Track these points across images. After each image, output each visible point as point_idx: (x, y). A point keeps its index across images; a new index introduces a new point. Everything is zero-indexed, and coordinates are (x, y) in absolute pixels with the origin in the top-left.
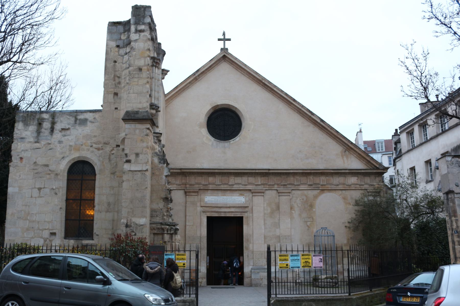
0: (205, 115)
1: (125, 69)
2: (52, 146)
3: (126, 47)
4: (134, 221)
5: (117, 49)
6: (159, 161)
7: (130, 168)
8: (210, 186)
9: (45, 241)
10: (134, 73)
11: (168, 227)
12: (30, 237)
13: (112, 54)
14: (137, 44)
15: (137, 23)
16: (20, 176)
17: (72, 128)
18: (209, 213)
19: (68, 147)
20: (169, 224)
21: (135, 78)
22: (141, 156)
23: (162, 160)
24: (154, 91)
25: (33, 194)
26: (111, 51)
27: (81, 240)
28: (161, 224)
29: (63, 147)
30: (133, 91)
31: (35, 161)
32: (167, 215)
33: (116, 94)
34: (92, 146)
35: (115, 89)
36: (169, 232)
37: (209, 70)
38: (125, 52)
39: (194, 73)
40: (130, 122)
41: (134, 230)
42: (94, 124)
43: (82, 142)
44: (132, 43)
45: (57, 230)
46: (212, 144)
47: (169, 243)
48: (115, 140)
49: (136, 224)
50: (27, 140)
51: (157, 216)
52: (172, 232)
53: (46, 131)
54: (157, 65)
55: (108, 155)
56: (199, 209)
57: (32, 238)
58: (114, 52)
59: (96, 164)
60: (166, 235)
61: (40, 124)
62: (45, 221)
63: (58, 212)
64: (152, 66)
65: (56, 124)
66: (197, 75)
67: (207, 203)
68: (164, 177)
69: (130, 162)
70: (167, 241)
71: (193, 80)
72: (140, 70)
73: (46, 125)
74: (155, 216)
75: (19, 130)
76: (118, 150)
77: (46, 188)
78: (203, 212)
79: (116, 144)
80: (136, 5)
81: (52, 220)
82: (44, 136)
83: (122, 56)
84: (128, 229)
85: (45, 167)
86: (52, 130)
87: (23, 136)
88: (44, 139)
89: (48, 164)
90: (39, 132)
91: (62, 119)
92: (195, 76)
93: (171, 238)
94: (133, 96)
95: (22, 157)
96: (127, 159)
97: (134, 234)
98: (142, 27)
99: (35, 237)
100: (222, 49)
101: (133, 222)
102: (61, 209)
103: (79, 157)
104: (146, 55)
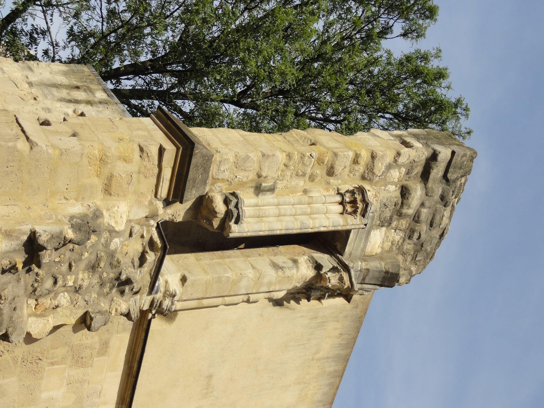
50: (29, 74)
54: (349, 208)
73: (80, 95)
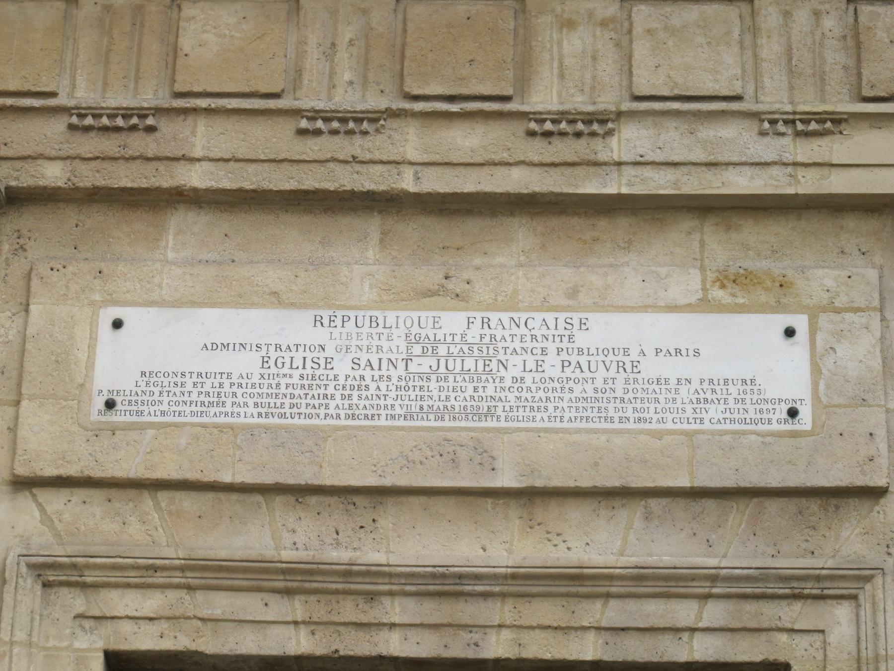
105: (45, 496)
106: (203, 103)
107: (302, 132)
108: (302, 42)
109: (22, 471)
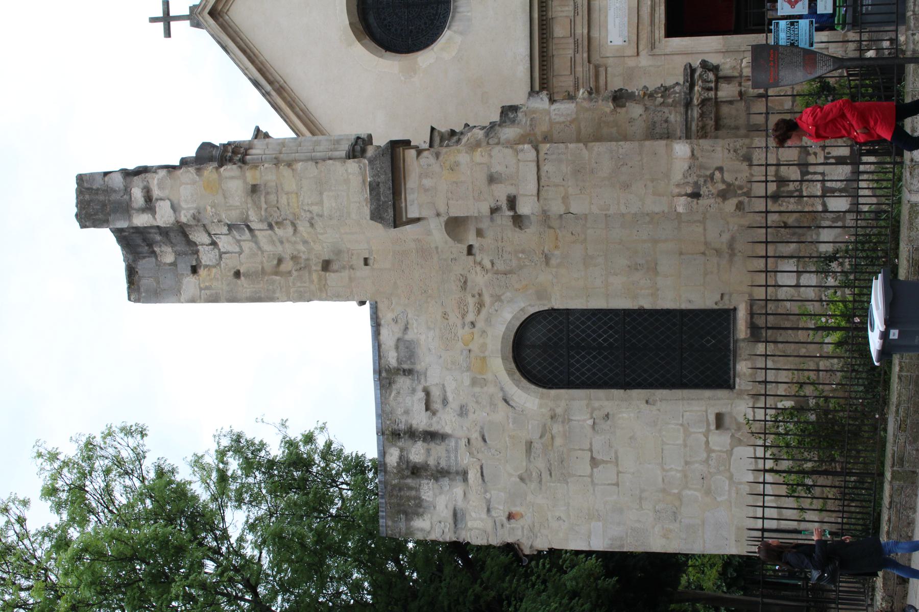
0: (380, 59)
1: (256, 243)
2: (475, 436)
3: (195, 244)
4: (681, 176)
5: (202, 272)
6: (508, 123)
7: (532, 195)
8: (579, 31)
9: (740, 442)
10: (264, 206)
11: (696, 88)
12: (729, 485)
13: (215, 284)
14: (184, 205)
15: (125, 209)
16: (559, 518)
17: (423, 381)
18: (657, 32)
19: (477, 389)
20: (688, 84)
21: (277, 201)
22: (497, 168)
23: (507, 114)
24: (313, 154)
25: (610, 482)
26: (207, 288)
27: (736, 341)
28: (688, 104)
29: (477, 402)
30: (317, 204)
31: (518, 480)
32: (662, 97)
33: (326, 265)
34: (473, 324)
35: (314, 268)
36: (713, 85)
37: (254, 55)
38: (210, 247)
39: (263, 95)
40: (401, 208)
41: (708, 173)
42: (410, 321)
43: (462, 351)
44: (184, 219)
45: (709, 411)
46: (461, 33)
47: (743, 84)
48: (456, 259)
49: (690, 168)
50: (460, 504)
51: (666, 121)
52: (711, 76)
53: (433, 452)
55: (496, 276)
56: (645, 60)
57: (731, 478)
58: (211, 279)
59: (522, 310)
60: (720, 94)
61: (416, 471)
62: (685, 446)
63: (659, 410)
64: (243, 161)
65: (414, 426)
66: (268, 88)
67: (627, 39)
68: (556, 106)
69: (515, 197)
70: (739, 89)
71: (284, 99)
72: (254, 189)
73: (417, 453)
74: (665, 125)
75: (432, 527)
76: (482, 249)
77: (591, 444)
78: (653, 46)
79: (464, 256)
80: (77, 215)
81: (682, 425)
82: (449, 457)
83: (221, 257)
84: (703, 191)
85: (533, 450)
86: (431, 436)
87: (447, 514)
88: (456, 457)
89: (524, 441)
90: (440, 474)
91: (400, 411)
92: (273, 93)
93: (728, 79)
94: (329, 204)
95: (507, 513)
96: (505, 207)
97: (717, 175)
98: (137, 194)
99: (729, 470)
100: (197, 24)
101: (685, 177)
102: (650, 401)
103: (504, 359)
104: (215, 176)
105: (639, 51)
106: (573, 31)
107: (578, 15)
108: (561, 17)
109: (636, 54)
